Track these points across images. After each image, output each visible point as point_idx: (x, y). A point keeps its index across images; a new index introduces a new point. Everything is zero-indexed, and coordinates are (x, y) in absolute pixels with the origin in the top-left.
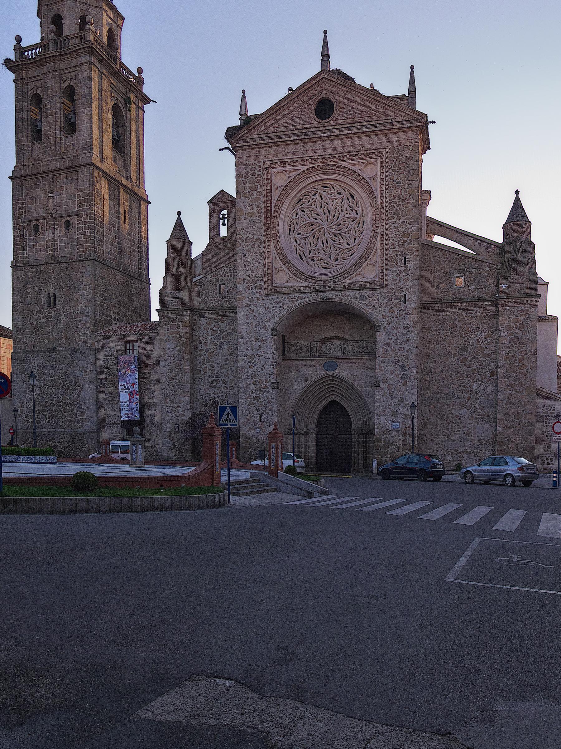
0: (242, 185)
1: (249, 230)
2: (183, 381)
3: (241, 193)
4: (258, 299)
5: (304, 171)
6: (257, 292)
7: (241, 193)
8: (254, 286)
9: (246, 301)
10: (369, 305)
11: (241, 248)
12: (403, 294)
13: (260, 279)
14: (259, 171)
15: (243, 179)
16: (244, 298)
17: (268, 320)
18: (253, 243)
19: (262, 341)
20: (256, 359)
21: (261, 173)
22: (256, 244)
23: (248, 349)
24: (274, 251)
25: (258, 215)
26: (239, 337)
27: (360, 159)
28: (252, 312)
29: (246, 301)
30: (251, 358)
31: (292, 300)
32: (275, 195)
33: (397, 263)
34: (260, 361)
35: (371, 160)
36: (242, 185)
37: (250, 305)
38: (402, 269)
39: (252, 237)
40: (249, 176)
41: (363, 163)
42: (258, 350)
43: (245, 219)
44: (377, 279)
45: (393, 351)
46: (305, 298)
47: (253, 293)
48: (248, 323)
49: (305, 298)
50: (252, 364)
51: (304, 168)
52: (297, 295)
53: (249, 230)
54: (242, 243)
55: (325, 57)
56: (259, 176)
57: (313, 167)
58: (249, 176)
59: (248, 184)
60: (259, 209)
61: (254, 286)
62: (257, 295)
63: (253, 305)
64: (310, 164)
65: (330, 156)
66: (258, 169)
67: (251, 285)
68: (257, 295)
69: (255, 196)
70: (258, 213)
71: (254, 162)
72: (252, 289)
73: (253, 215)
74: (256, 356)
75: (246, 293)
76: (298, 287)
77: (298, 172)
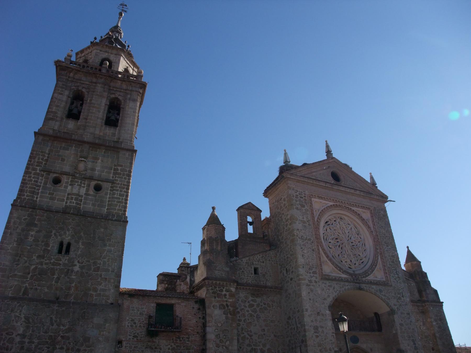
0: (294, 201)
1: (303, 231)
2: (230, 348)
3: (295, 207)
4: (316, 282)
5: (331, 206)
6: (314, 276)
7: (295, 207)
8: (311, 272)
9: (307, 282)
10: (385, 296)
11: (298, 242)
12: (401, 291)
13: (315, 267)
14: (305, 197)
15: (295, 198)
16: (305, 279)
17: (325, 299)
18: (307, 241)
19: (323, 315)
20: (320, 329)
21: (306, 198)
22: (309, 242)
23: (312, 321)
24: (321, 250)
25: (308, 223)
26: (304, 310)
27: (361, 208)
28: (312, 291)
29: (307, 282)
30: (316, 328)
31: (339, 286)
32: (316, 214)
33: (393, 272)
34: (323, 332)
35: (366, 211)
36: (294, 201)
37: (310, 285)
38: (396, 276)
39: (306, 237)
40: (298, 198)
41: (362, 211)
42: (320, 322)
43: (299, 223)
44: (384, 280)
45: (405, 330)
46: (347, 285)
47: (312, 277)
48: (310, 299)
49: (347, 285)
50: (317, 334)
51: (331, 204)
52: (342, 283)
53: (303, 231)
54: (299, 239)
55: (329, 152)
56: (305, 200)
57: (336, 205)
58: (298, 198)
59: (298, 202)
60: (308, 219)
61: (311, 272)
62: (313, 279)
63: (312, 285)
64: (335, 202)
65: (346, 202)
66: (304, 195)
67: (309, 271)
68: (313, 279)
69: (304, 211)
70: (308, 222)
71: (301, 191)
72: (310, 273)
73: (304, 222)
74: (319, 328)
75: (306, 275)
76: (340, 277)
77: (329, 205)
